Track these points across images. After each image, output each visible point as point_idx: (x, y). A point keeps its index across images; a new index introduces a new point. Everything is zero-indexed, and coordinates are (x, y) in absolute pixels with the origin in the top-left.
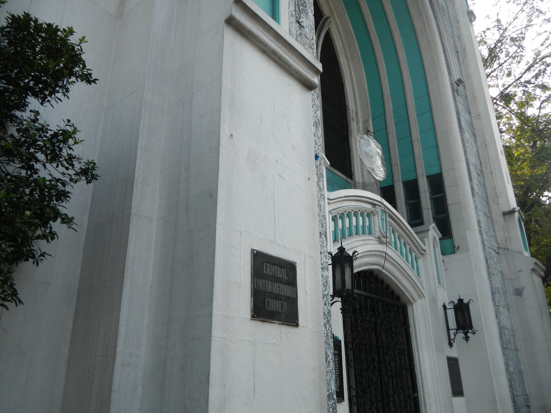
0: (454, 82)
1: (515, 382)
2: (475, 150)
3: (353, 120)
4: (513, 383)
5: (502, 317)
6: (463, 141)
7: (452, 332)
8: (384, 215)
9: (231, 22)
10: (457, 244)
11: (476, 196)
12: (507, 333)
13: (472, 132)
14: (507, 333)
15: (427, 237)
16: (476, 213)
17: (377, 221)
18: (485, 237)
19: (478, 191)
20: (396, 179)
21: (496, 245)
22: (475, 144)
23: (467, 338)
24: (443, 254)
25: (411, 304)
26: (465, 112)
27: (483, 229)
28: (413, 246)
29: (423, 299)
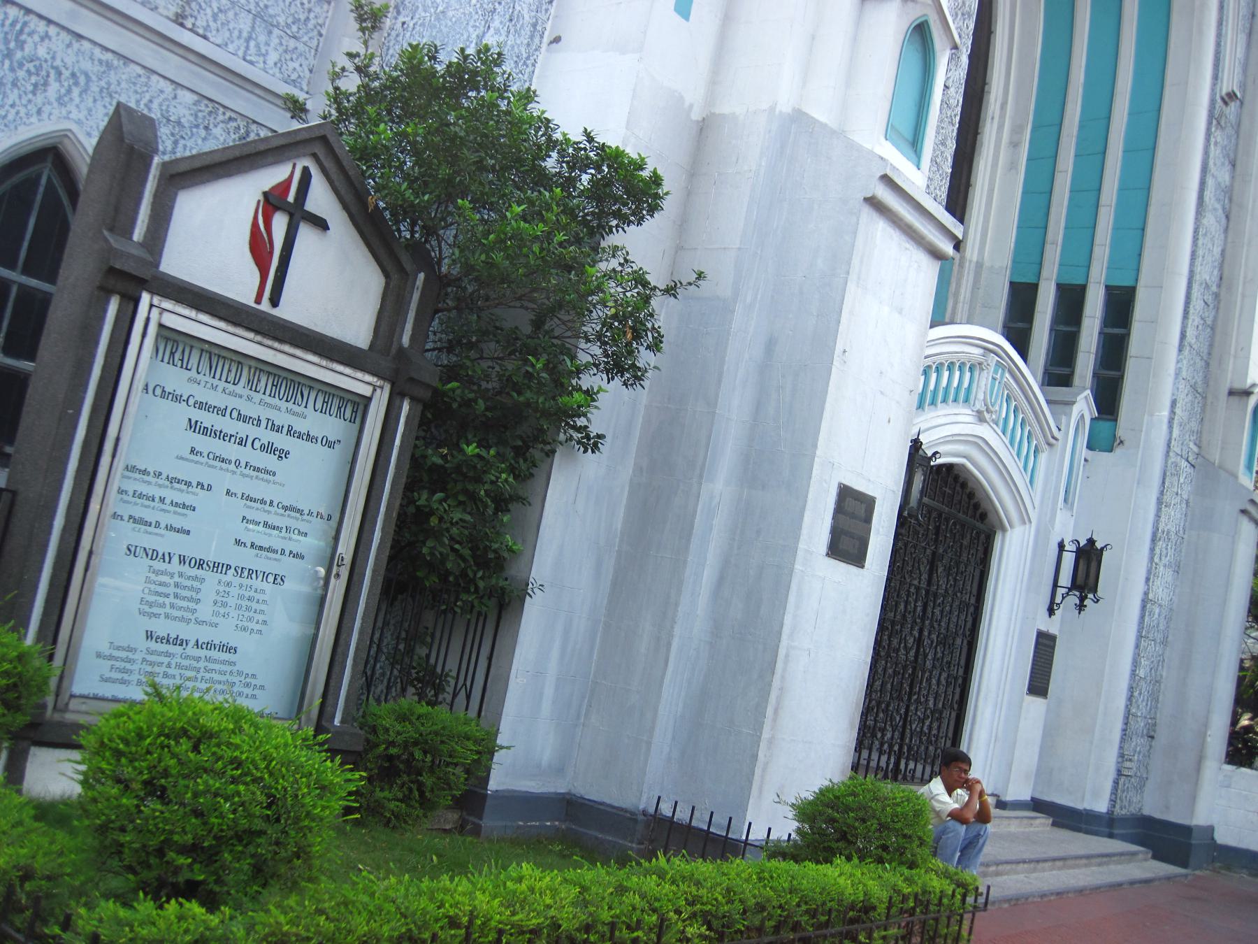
0: (1218, 98)
1: (1140, 694)
2: (1217, 251)
3: (993, 118)
4: (1136, 694)
5: (1158, 582)
6: (1196, 231)
7: (1060, 591)
8: (1000, 371)
9: (873, 202)
10: (1120, 433)
11: (1186, 352)
12: (1157, 611)
13: (1224, 209)
14: (1157, 611)
15: (1069, 415)
16: (1175, 384)
17: (983, 383)
18: (1176, 432)
19: (1193, 341)
20: (1044, 274)
21: (1195, 449)
22: (1222, 236)
23: (1081, 607)
24: (1090, 447)
25: (1004, 530)
26: (1223, 164)
27: (1176, 418)
28: (1037, 428)
29: (1027, 526)
